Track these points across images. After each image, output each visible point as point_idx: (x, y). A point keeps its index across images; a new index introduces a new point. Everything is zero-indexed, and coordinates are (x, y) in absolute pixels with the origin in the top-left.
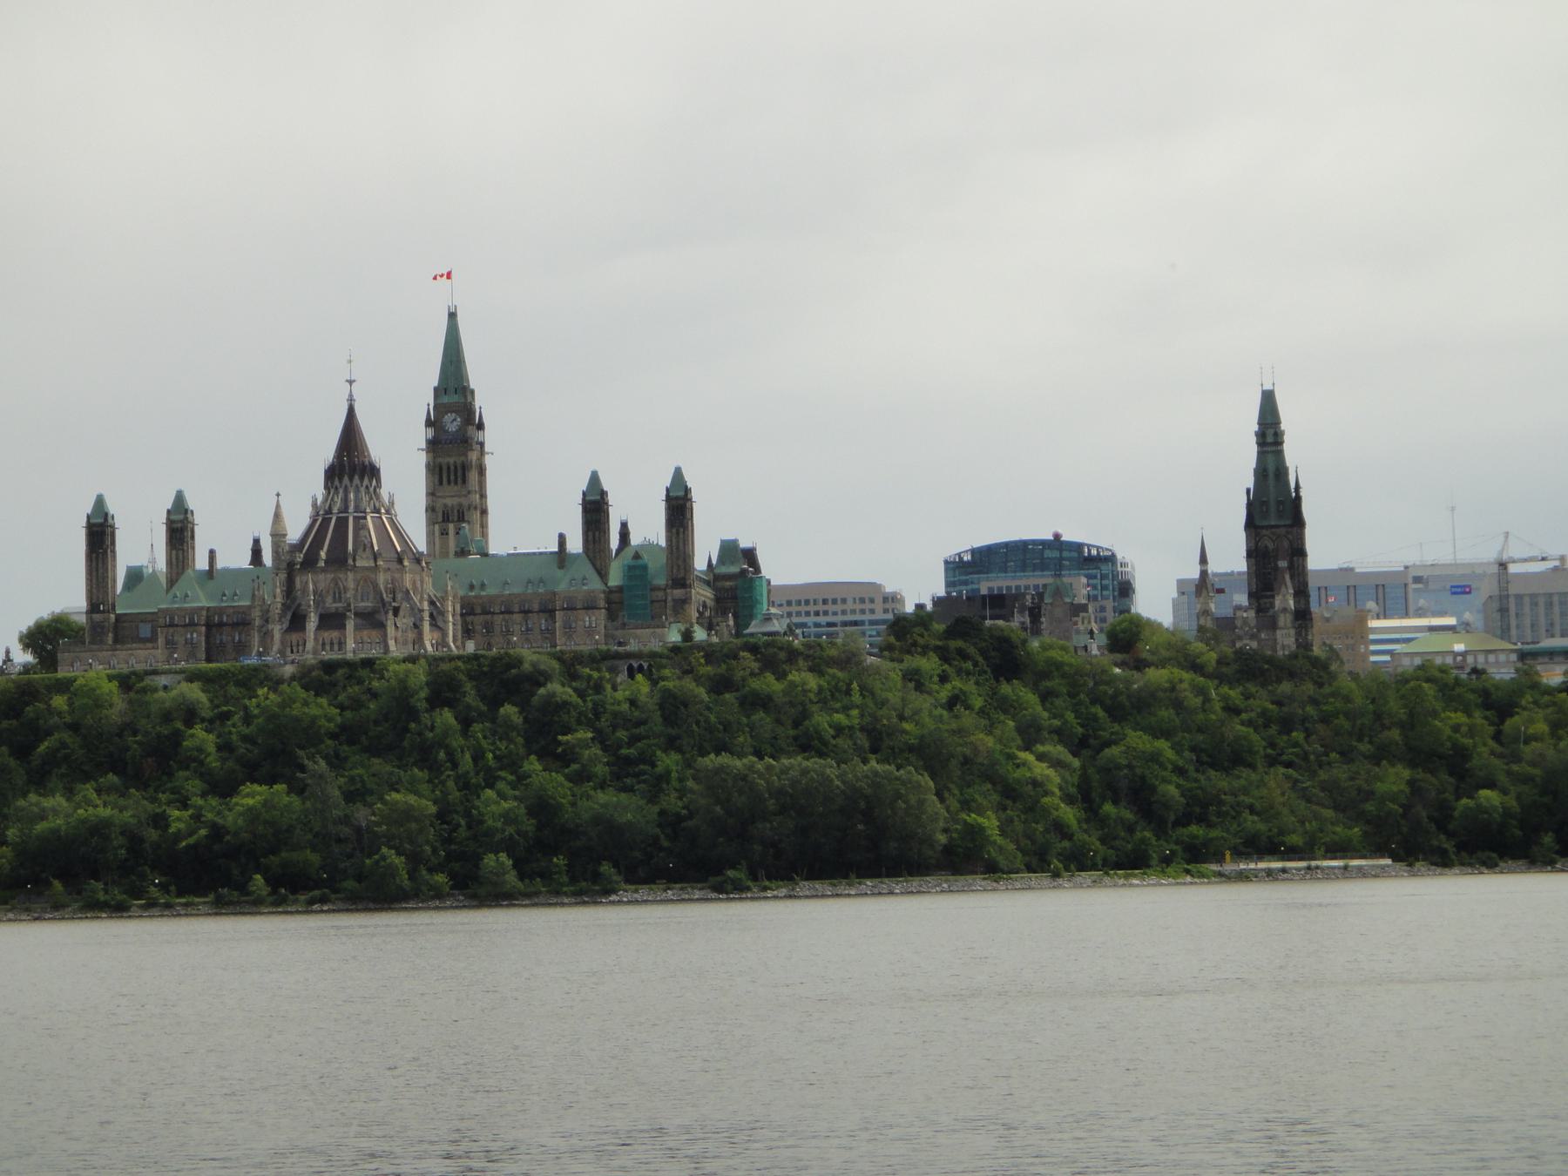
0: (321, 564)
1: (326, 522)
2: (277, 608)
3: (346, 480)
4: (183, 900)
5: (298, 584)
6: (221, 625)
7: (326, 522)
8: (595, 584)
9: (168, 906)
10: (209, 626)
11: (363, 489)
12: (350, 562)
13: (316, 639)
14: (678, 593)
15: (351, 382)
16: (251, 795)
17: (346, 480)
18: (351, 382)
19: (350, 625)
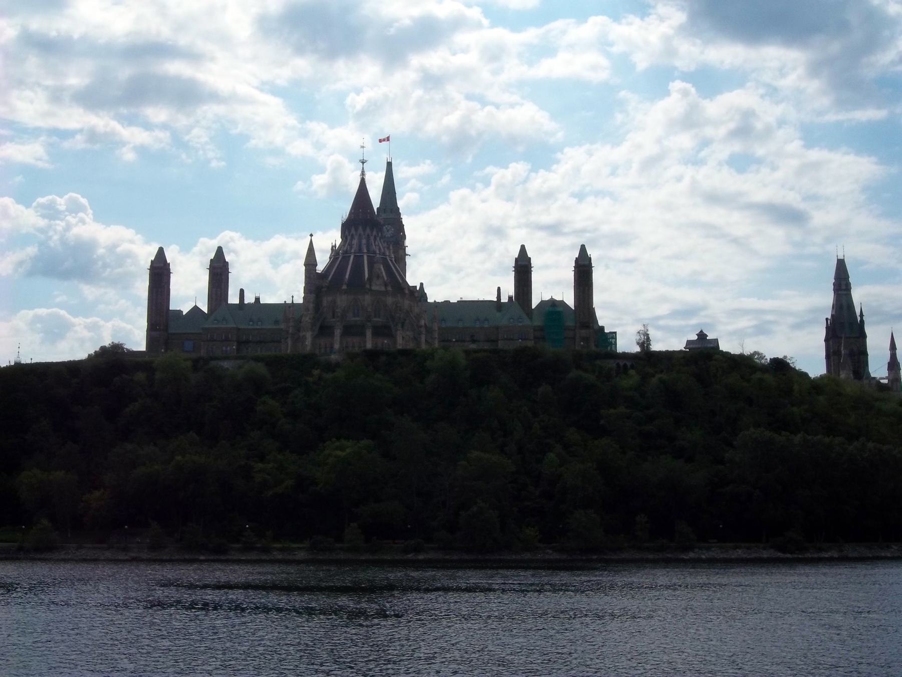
0: (344, 287)
1: (345, 258)
2: (307, 319)
3: (360, 230)
4: (278, 546)
5: (325, 303)
6: (247, 342)
7: (345, 258)
8: (527, 322)
9: (266, 550)
10: (240, 343)
11: (372, 238)
12: (368, 286)
13: (341, 343)
14: (584, 332)
15: (363, 163)
16: (342, 449)
17: (360, 230)
18: (363, 163)
19: (369, 333)
